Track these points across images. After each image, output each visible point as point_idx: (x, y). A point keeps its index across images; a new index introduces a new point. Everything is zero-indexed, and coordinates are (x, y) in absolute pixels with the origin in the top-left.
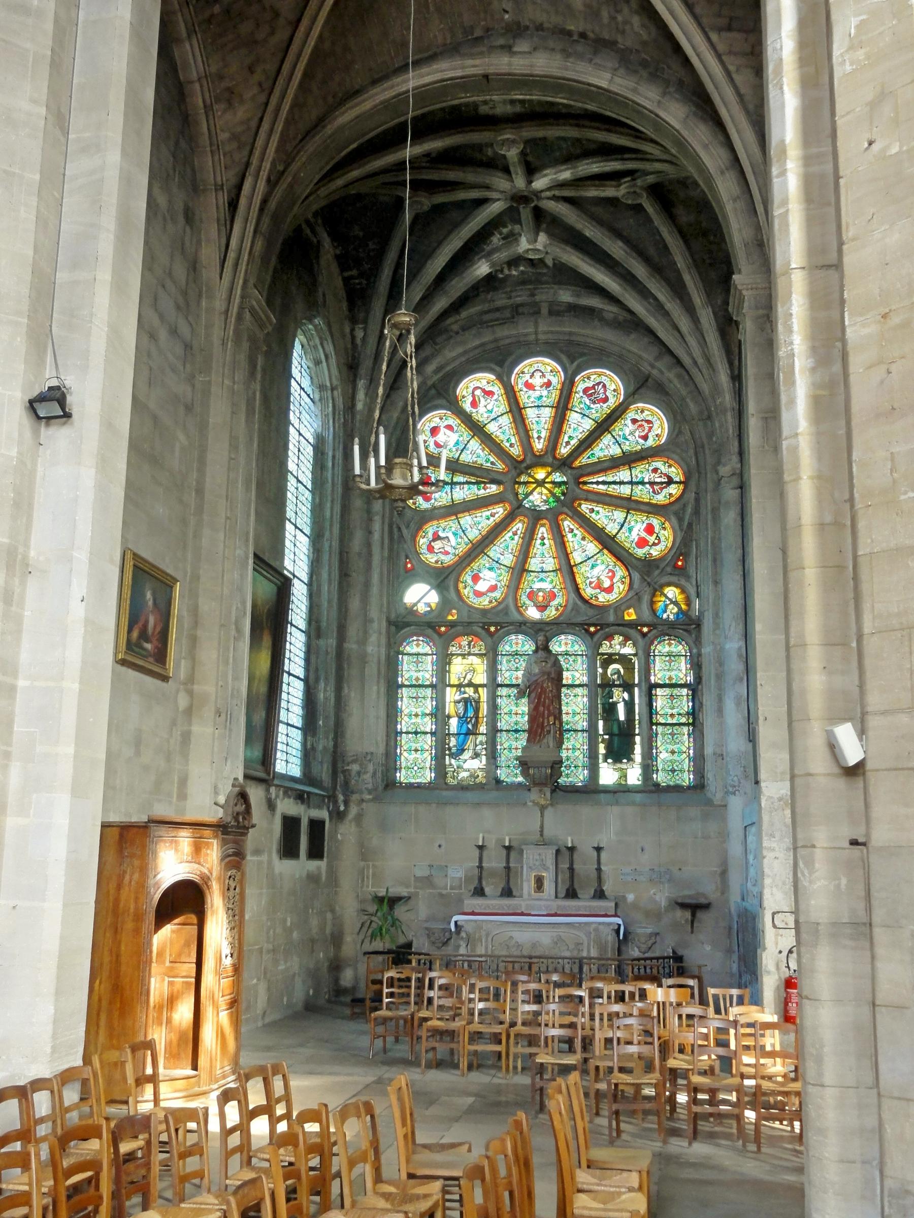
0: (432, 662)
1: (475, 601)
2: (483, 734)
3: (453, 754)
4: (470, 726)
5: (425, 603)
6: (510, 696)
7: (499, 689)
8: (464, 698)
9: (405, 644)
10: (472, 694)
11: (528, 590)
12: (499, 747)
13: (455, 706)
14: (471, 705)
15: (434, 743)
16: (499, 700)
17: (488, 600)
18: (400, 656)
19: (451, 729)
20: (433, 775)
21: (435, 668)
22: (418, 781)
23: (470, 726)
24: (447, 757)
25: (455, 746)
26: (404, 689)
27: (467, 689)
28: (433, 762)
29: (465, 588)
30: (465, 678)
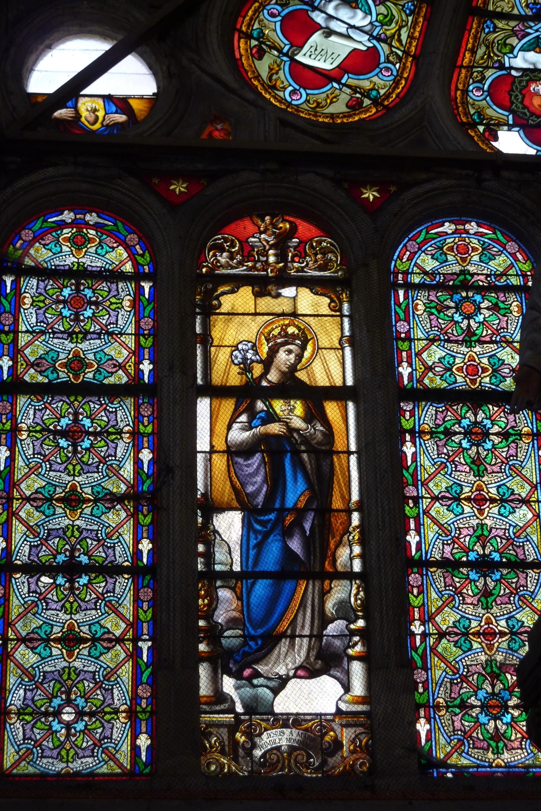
0: (136, 304)
1: (300, 99)
2: (349, 576)
3: (230, 653)
4: (295, 545)
5: (108, 98)
6: (449, 433)
7: (407, 407)
8: (266, 438)
9: (27, 235)
10: (297, 423)
11: (491, 75)
12: (417, 628)
13: (231, 464)
14: (298, 464)
15: (146, 614)
16: (409, 449)
17: (345, 96)
18: (9, 280)
19: (220, 555)
20: (144, 741)
21: (147, 324)
22: (76, 766)
23: (295, 545)
24: (204, 671)
25: (233, 623)
26: (22, 401)
27: (278, 406)
28: (144, 692)
29: (260, 54)
30: (268, 363)
